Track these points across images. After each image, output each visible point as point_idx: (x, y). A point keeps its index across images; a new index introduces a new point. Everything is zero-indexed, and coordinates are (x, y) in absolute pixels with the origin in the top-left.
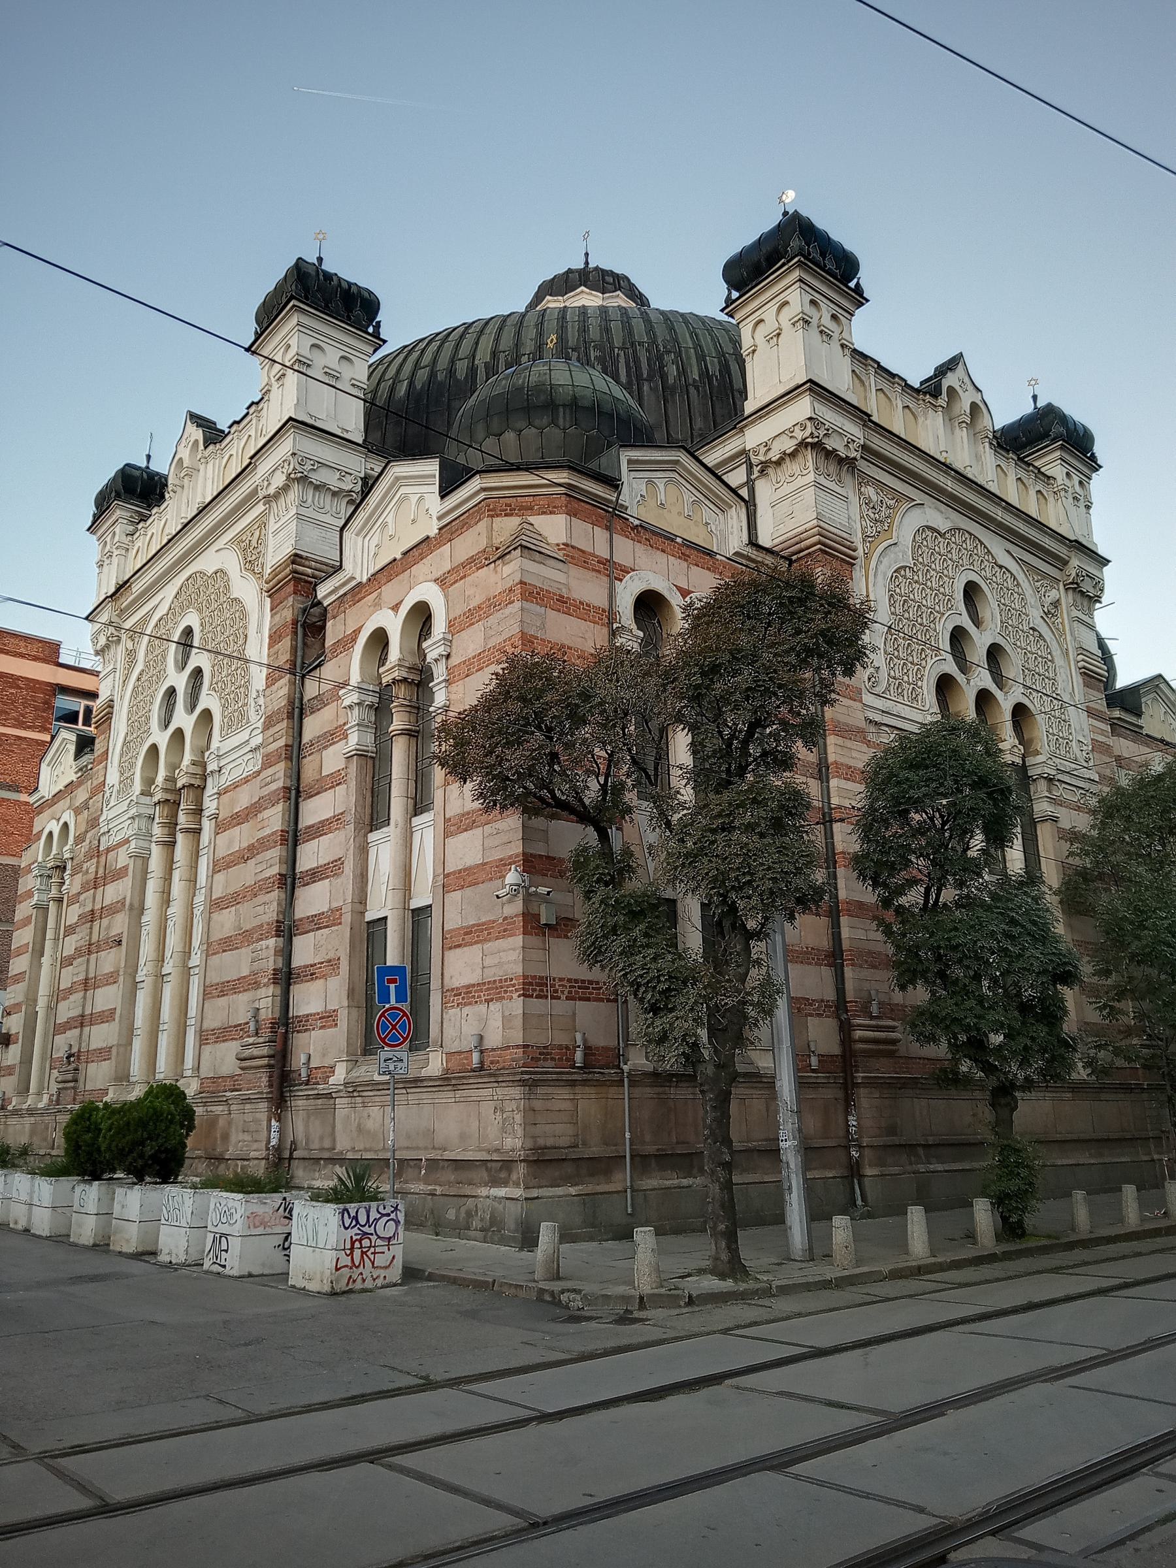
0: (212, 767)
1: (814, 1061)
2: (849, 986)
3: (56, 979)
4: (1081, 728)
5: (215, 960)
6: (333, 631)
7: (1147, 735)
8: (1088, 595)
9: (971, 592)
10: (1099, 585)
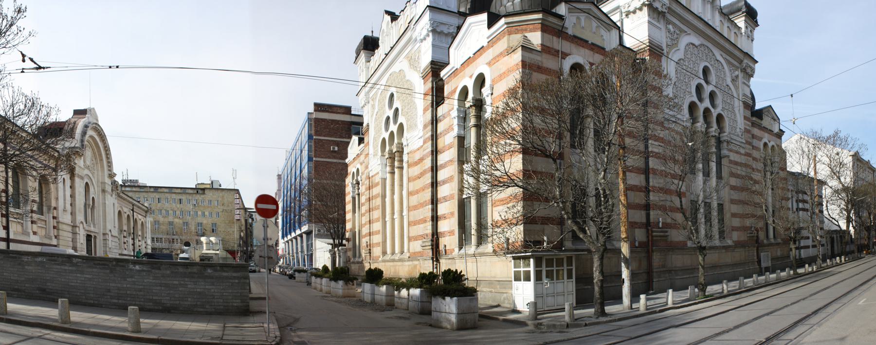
0: (405, 143)
1: (637, 244)
2: (652, 217)
3: (360, 221)
5: (411, 213)
6: (447, 90)
9: (706, 71)
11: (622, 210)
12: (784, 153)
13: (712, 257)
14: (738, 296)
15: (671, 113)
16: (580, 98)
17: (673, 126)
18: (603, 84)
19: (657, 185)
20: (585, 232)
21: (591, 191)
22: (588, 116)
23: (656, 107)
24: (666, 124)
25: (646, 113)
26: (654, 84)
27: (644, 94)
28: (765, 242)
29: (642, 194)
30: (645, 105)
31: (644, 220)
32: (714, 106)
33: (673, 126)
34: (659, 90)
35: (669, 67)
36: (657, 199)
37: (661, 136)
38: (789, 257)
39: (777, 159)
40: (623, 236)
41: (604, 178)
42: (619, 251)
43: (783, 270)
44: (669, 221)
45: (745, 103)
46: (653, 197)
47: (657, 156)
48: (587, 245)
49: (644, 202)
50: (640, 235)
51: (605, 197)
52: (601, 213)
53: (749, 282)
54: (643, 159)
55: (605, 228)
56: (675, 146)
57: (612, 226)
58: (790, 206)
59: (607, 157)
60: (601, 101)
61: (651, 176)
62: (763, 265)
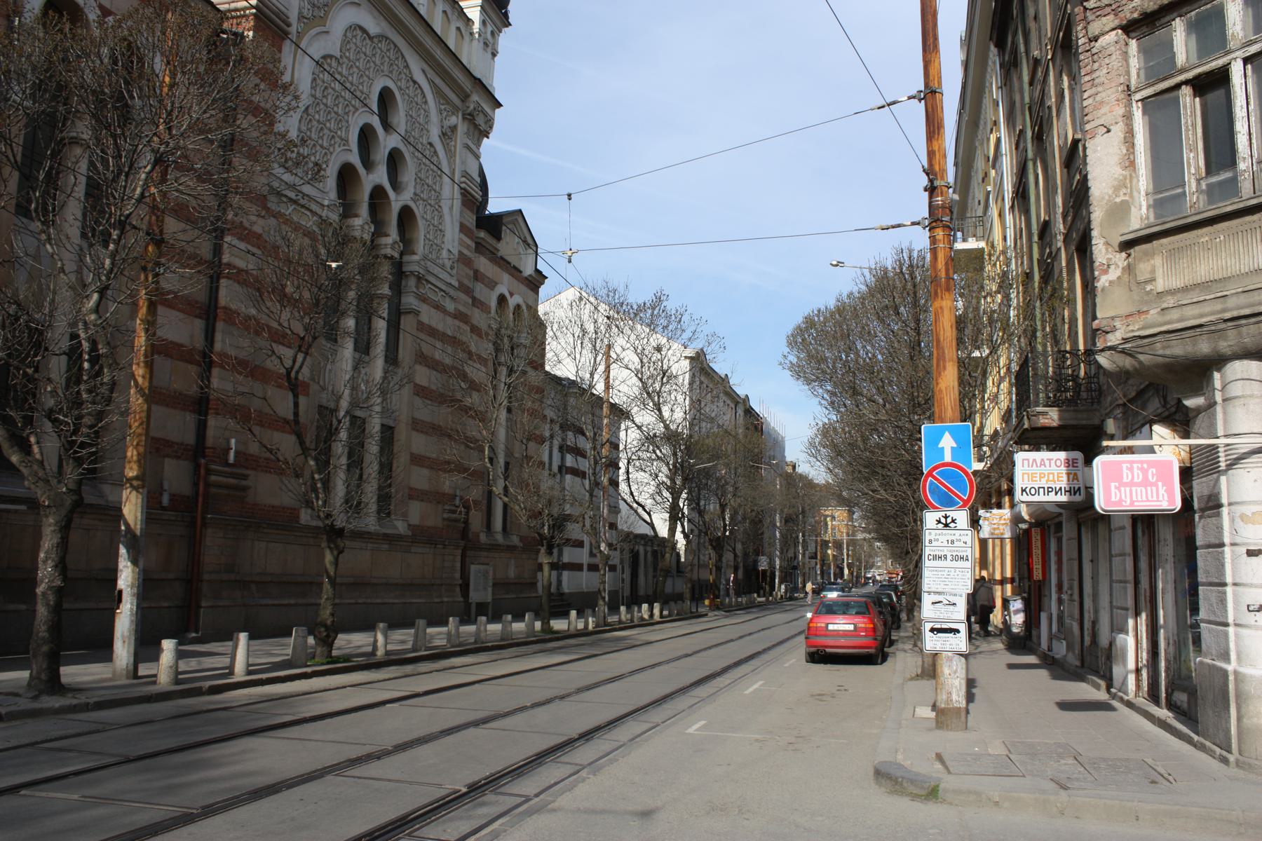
1: (165, 500)
2: (211, 433)
4: (452, 240)
7: (502, 258)
8: (480, 128)
9: (386, 98)
10: (490, 122)
11: (137, 401)
12: (539, 327)
13: (357, 559)
14: (409, 669)
15: (287, 177)
16: (61, 87)
17: (288, 210)
18: (128, 68)
19: (233, 352)
20: (25, 448)
21: (58, 338)
22: (75, 141)
23: (253, 155)
24: (273, 204)
25: (227, 164)
26: (256, 98)
27: (229, 117)
28: (483, 538)
29: (193, 370)
30: (229, 144)
31: (190, 438)
32: (396, 185)
33: (288, 210)
34: (267, 118)
35: (299, 70)
36: (229, 387)
37: (257, 229)
38: (533, 585)
39: (524, 339)
40: (132, 471)
41: (97, 310)
42: (115, 513)
43: (519, 617)
44: (254, 448)
45: (465, 193)
46: (219, 381)
47: (240, 276)
48: (29, 486)
49: (194, 390)
50: (176, 476)
51: (94, 362)
52: (77, 403)
53: (438, 635)
54: (205, 280)
55: (83, 445)
56: (289, 261)
57: (105, 441)
58: (546, 459)
59: (113, 256)
60: (115, 112)
61: (220, 325)
62: (475, 596)
